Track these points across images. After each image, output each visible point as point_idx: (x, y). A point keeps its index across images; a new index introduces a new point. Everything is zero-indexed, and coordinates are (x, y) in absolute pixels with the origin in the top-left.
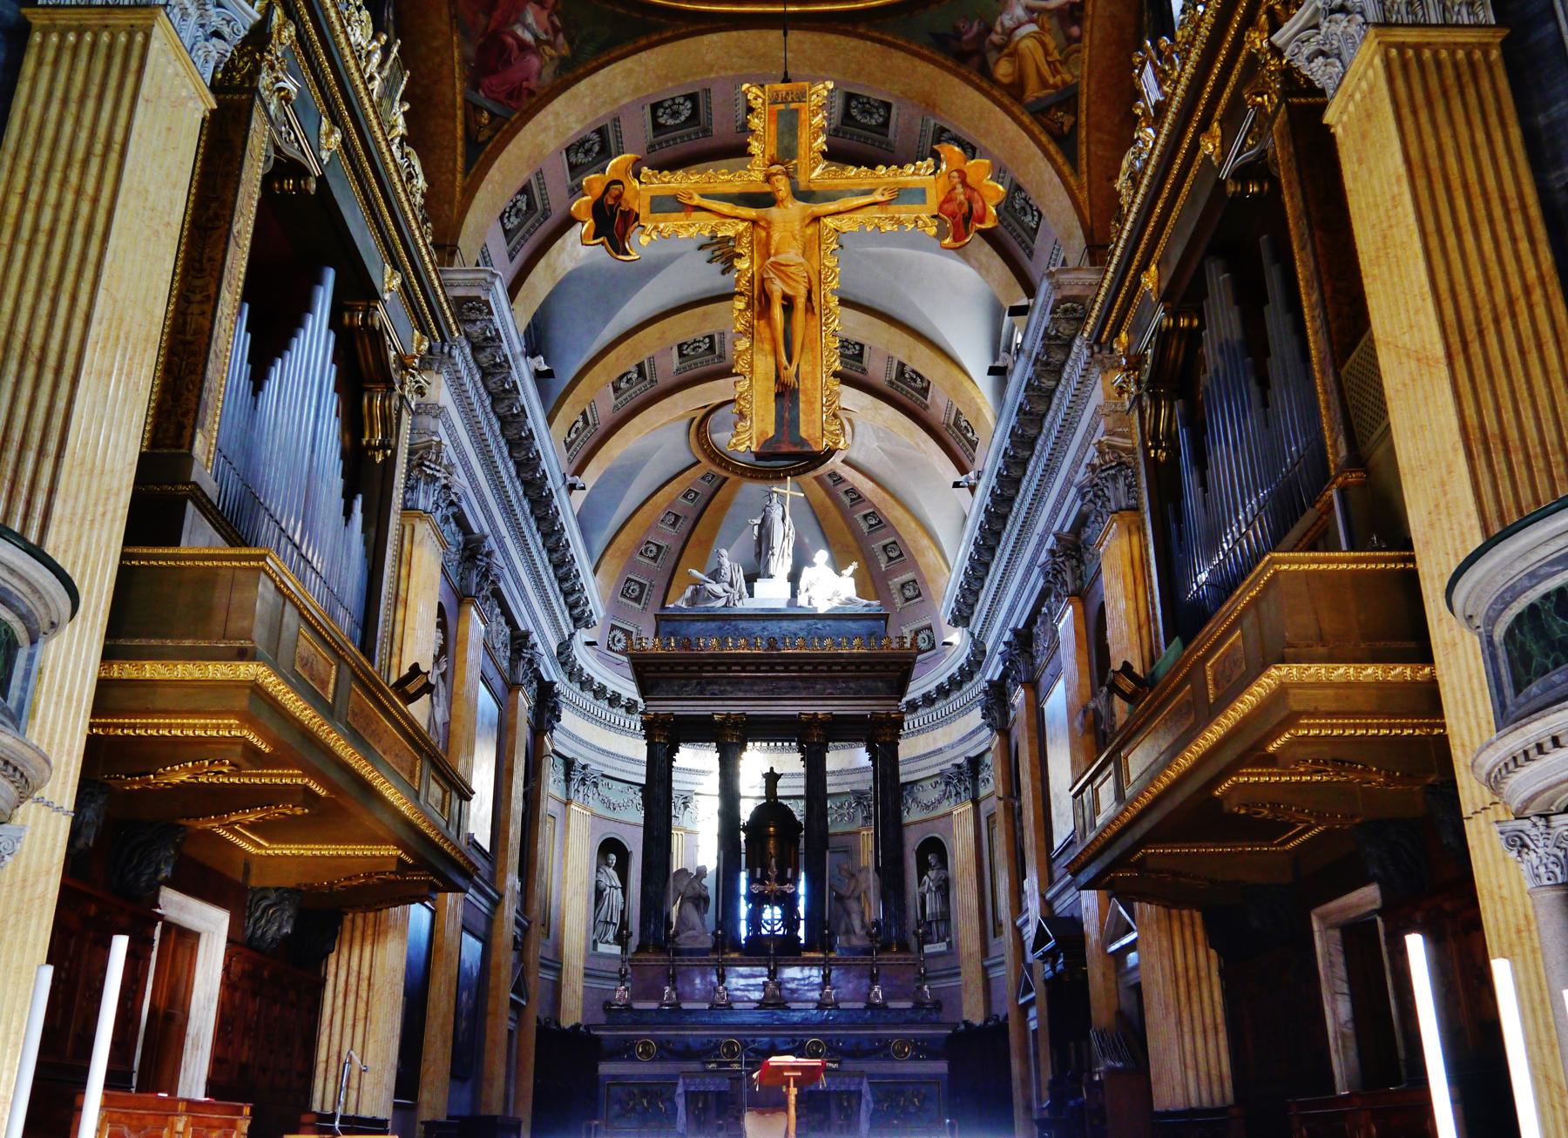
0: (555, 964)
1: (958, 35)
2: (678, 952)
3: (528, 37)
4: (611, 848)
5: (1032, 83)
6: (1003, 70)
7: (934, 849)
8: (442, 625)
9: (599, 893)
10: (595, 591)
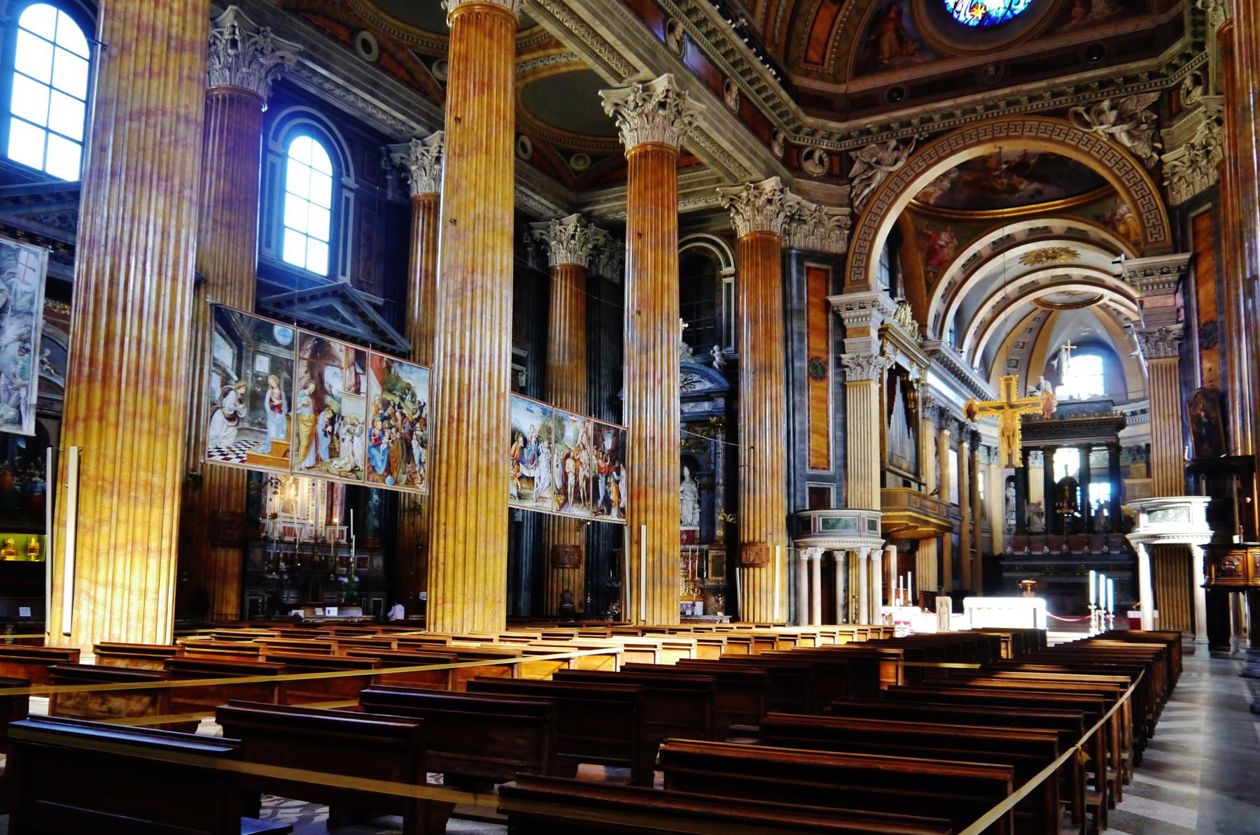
0: (990, 530)
1: (1103, 216)
2: (1032, 534)
3: (942, 243)
5: (1132, 234)
6: (1122, 229)
8: (936, 444)
9: (1007, 500)
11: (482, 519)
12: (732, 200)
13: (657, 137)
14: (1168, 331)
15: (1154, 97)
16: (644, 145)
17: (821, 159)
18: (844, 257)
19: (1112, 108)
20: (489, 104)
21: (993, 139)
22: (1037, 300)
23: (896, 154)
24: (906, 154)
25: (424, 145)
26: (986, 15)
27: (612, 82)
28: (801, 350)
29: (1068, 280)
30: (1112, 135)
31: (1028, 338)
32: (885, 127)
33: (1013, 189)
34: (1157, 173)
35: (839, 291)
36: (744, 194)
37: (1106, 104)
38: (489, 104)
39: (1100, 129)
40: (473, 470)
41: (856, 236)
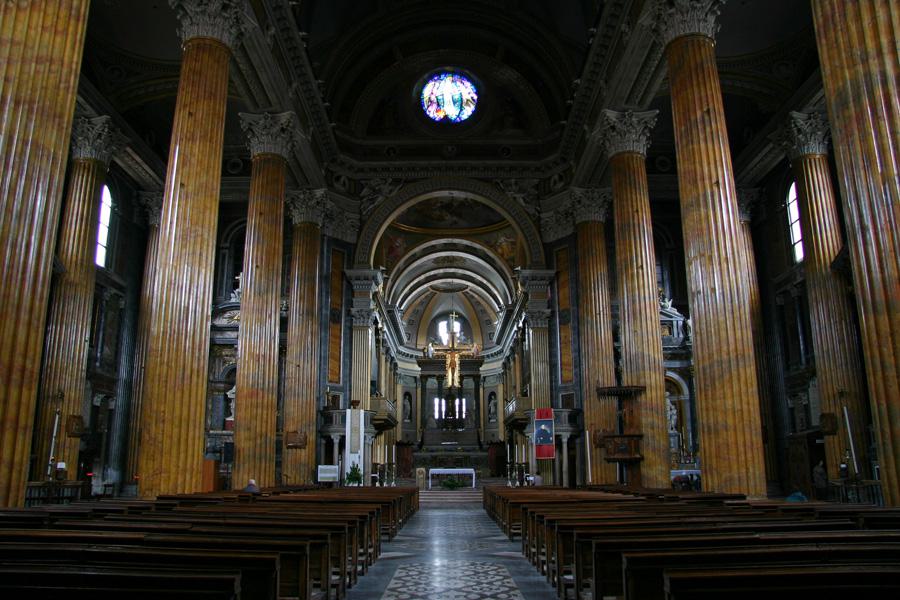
4: (407, 395)
6: (500, 251)
7: (493, 395)
10: (402, 324)
11: (192, 409)
12: (293, 199)
13: (278, 152)
14: (543, 313)
15: (536, 181)
16: (267, 154)
17: (344, 183)
18: (356, 245)
19: (516, 184)
20: (214, 109)
21: (450, 189)
22: (431, 286)
23: (390, 188)
24: (398, 188)
25: (89, 123)
26: (446, 117)
27: (251, 109)
28: (327, 302)
29: (453, 276)
30: (515, 198)
31: (421, 308)
32: (386, 169)
33: (441, 219)
34: (538, 221)
35: (350, 267)
36: (302, 196)
37: (513, 181)
38: (214, 109)
39: (509, 194)
40: (188, 372)
41: (363, 234)
